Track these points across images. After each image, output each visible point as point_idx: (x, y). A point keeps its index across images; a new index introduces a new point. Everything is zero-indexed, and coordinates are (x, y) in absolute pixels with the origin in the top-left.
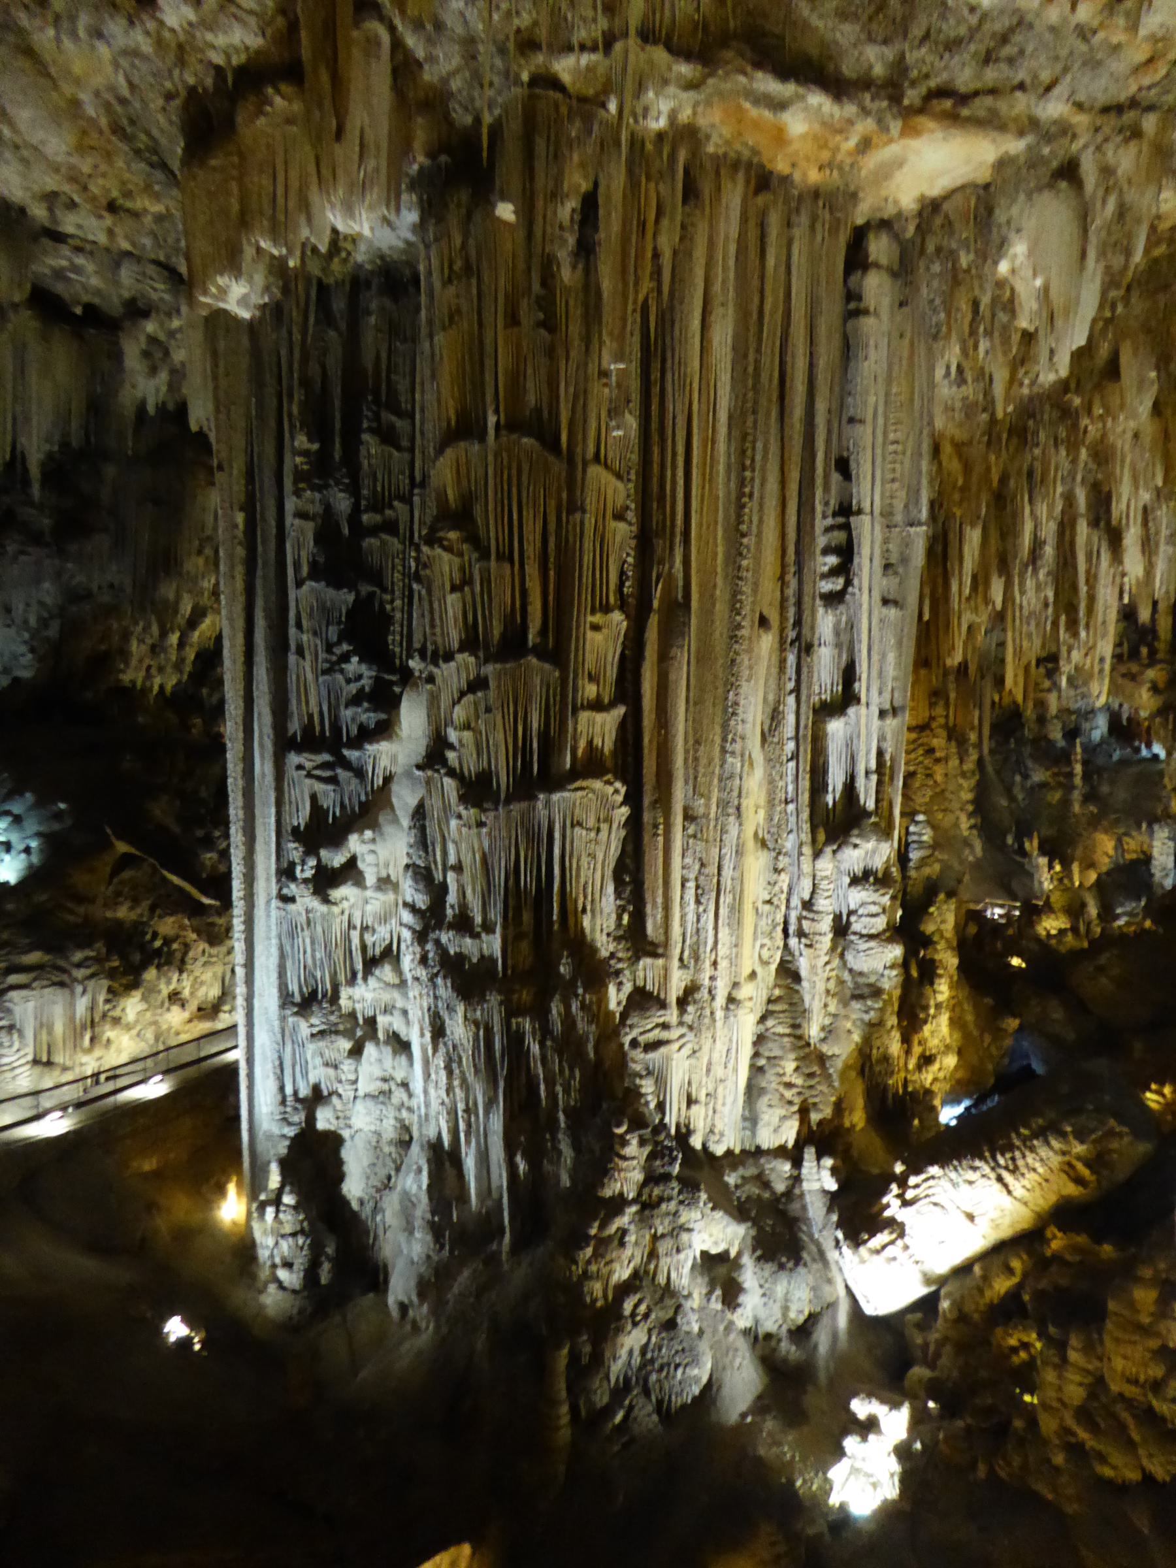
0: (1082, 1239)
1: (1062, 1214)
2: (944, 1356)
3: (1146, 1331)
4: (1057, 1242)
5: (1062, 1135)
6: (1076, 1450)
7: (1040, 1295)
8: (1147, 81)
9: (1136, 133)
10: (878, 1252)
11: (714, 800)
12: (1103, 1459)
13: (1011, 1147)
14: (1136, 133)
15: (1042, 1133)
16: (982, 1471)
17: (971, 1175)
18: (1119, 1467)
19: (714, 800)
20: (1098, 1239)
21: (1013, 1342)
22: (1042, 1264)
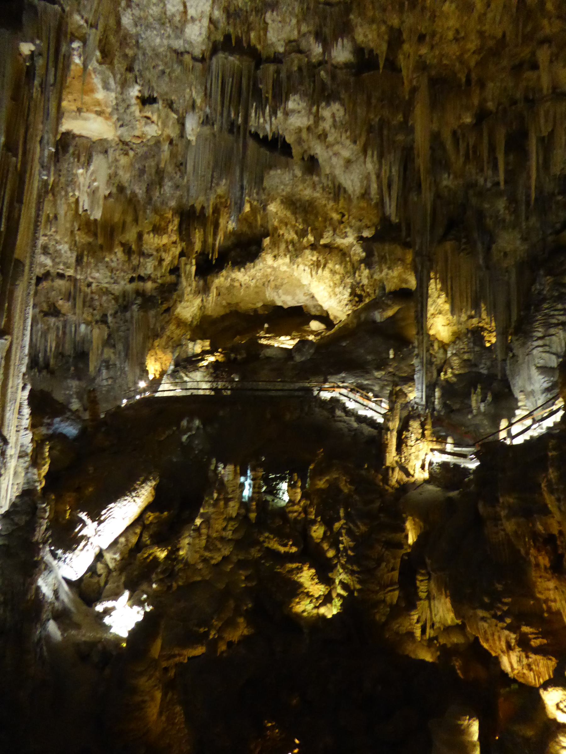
0: (157, 514)
1: (149, 508)
2: (131, 568)
3: (222, 513)
4: (151, 517)
5: (150, 480)
6: (205, 560)
7: (151, 537)
8: (134, 141)
9: (127, 154)
10: (82, 550)
11: (18, 356)
12: (212, 558)
13: (135, 489)
14: (127, 154)
15: (143, 482)
16: (174, 585)
17: (125, 502)
18: (218, 558)
19: (18, 356)
20: (162, 512)
21: (146, 555)
22: (145, 527)
